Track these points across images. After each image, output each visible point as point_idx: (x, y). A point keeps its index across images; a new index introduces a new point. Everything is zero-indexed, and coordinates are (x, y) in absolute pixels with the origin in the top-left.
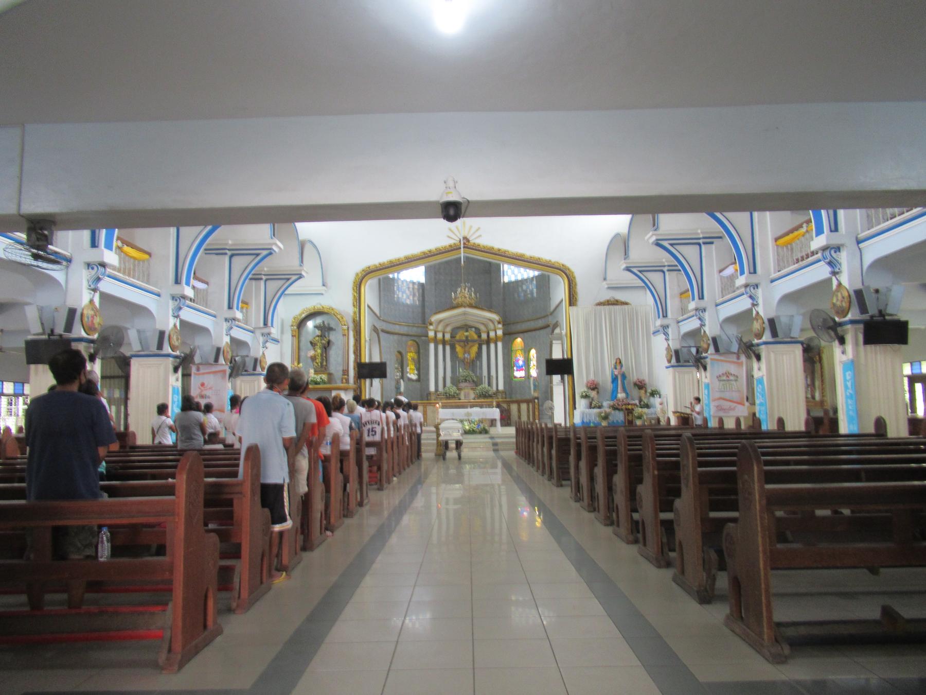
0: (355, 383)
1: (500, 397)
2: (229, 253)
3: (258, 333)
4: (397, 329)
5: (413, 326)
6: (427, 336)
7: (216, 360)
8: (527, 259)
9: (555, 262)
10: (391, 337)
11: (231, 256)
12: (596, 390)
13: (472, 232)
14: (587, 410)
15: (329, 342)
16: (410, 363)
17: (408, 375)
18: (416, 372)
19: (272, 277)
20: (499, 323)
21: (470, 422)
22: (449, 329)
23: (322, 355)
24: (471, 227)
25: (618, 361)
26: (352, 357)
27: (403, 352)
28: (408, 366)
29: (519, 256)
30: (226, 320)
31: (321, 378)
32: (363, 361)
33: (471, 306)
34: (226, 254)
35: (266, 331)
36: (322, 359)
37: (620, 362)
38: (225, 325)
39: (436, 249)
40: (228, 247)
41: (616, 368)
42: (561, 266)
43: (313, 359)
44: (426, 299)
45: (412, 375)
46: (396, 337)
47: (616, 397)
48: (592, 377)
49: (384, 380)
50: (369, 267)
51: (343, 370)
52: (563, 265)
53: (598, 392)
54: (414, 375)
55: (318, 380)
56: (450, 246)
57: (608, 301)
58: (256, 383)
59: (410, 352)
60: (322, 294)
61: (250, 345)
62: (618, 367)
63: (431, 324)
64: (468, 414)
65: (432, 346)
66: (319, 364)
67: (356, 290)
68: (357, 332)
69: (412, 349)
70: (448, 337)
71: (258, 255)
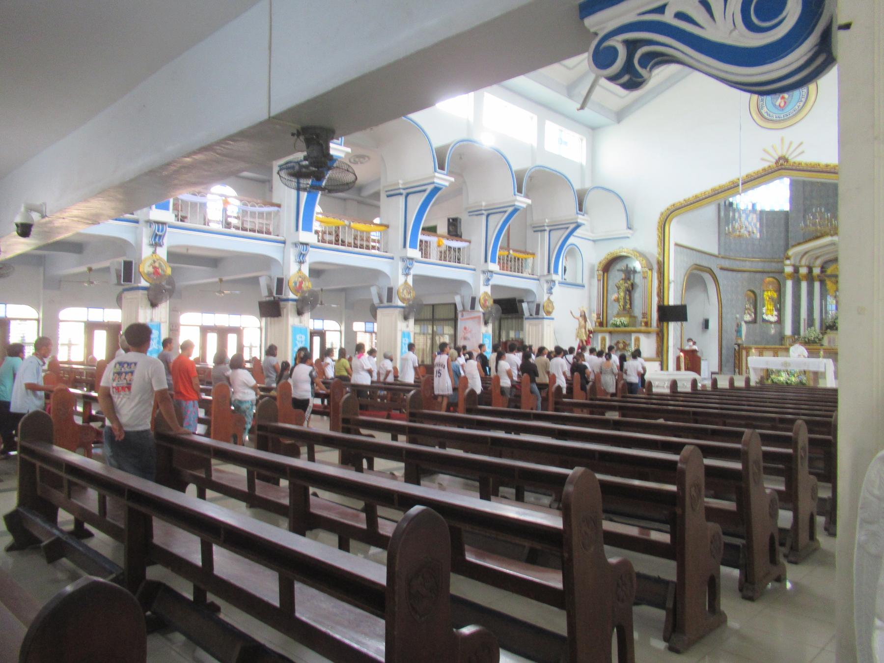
0: (658, 326)
2: (485, 213)
3: (543, 280)
4: (747, 266)
5: (771, 262)
6: (782, 272)
7: (473, 307)
10: (739, 275)
11: (488, 216)
13: (791, 149)
15: (632, 285)
16: (766, 302)
17: (764, 316)
18: (775, 313)
19: (554, 227)
21: (789, 373)
22: (819, 262)
23: (625, 298)
24: (791, 143)
26: (655, 300)
27: (757, 291)
28: (764, 306)
30: (484, 272)
31: (621, 321)
32: (666, 303)
34: (482, 214)
35: (548, 278)
36: (625, 303)
38: (482, 278)
39: (747, 176)
40: (483, 208)
43: (617, 300)
46: (746, 275)
49: (684, 323)
50: (674, 205)
51: (643, 313)
54: (772, 316)
55: (618, 323)
56: (764, 170)
58: (540, 326)
59: (767, 291)
60: (628, 237)
61: (536, 293)
63: (788, 258)
64: (786, 364)
65: (789, 284)
66: (622, 307)
67: (660, 230)
68: (661, 273)
69: (771, 287)
70: (817, 271)
71: (505, 212)
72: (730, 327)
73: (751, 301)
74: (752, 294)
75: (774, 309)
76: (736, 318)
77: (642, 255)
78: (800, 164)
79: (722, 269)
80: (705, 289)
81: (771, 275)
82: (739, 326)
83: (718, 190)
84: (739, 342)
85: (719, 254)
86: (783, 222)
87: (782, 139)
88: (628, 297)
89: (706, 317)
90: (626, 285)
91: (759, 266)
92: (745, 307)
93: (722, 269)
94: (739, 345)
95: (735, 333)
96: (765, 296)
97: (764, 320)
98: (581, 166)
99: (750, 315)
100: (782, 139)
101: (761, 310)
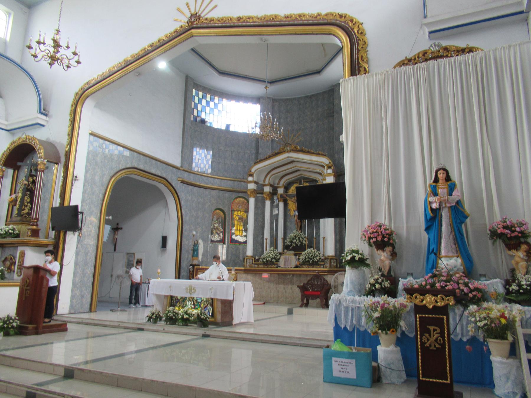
1: (327, 265)
5: (241, 181)
8: (281, 21)
9: (326, 15)
12: (388, 249)
14: (357, 298)
16: (236, 222)
17: (233, 237)
20: (329, 167)
21: (196, 303)
25: (441, 175)
27: (226, 210)
28: (234, 227)
29: (267, 21)
33: (297, 151)
37: (448, 178)
39: (159, 41)
41: (435, 194)
42: (338, 18)
44: (260, 152)
45: (239, 237)
46: (214, 192)
47: (435, 266)
48: (383, 219)
52: (341, 16)
53: (394, 255)
54: (241, 236)
56: (176, 31)
57: (425, 53)
59: (237, 211)
60: (43, 126)
62: (442, 190)
64: (191, 289)
69: (241, 207)
72: (188, 244)
73: (220, 221)
74: (222, 214)
75: (243, 229)
76: (193, 235)
77: (50, 146)
78: (212, 20)
79: (183, 182)
80: (166, 205)
81: (240, 195)
82: (196, 244)
84: (195, 262)
85: (181, 167)
86: (254, 144)
88: (27, 199)
89: (164, 235)
90: (26, 182)
91: (228, 185)
92: (214, 226)
93: (183, 182)
94: (193, 266)
95: (191, 252)
96: (235, 216)
97: (233, 241)
98: (5, 42)
99: (218, 234)
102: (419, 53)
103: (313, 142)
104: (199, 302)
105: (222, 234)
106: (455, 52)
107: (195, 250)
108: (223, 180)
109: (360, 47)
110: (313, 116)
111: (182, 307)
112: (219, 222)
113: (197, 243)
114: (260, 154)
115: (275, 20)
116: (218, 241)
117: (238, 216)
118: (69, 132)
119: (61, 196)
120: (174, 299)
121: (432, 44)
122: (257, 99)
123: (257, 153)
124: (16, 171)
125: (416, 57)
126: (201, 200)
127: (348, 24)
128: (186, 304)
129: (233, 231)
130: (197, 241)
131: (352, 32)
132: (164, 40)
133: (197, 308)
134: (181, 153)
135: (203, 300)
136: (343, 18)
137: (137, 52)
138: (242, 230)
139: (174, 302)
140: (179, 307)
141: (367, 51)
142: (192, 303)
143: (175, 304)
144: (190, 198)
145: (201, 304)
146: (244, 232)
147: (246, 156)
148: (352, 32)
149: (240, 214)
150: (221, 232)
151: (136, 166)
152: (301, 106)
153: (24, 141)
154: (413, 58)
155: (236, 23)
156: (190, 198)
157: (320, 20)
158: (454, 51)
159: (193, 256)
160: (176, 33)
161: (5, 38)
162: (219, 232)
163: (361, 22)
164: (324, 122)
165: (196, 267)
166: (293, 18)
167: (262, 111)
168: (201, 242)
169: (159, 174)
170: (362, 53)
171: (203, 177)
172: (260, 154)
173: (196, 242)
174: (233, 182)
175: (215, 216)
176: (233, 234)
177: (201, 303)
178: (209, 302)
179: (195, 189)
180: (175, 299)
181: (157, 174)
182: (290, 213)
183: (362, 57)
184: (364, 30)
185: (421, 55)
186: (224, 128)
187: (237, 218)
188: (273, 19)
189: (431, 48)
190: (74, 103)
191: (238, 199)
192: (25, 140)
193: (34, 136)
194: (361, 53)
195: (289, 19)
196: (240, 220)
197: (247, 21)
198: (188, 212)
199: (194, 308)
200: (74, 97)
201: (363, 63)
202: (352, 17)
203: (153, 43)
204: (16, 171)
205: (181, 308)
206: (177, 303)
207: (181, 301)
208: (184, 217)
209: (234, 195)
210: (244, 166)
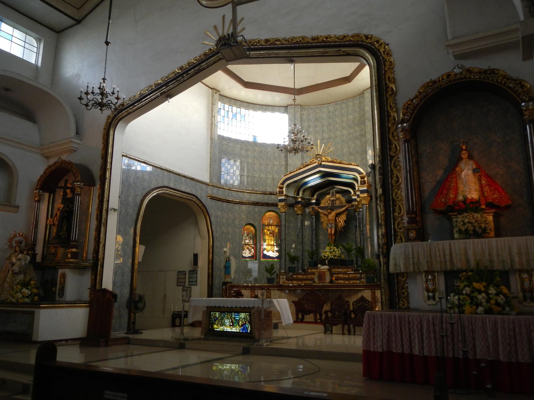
8: (308, 42)
9: (352, 37)
16: (267, 237)
17: (265, 252)
18: (276, 249)
27: (256, 224)
28: (265, 241)
39: (188, 64)
44: (289, 163)
46: (244, 207)
54: (273, 252)
56: (205, 54)
72: (219, 262)
73: (251, 236)
75: (275, 244)
76: (225, 252)
79: (213, 198)
81: (271, 208)
82: (228, 261)
83: (161, 83)
84: (228, 280)
87: (224, 17)
95: (223, 270)
97: (265, 256)
100: (224, 17)
101: (261, 245)
102: (443, 76)
103: (345, 150)
104: (237, 320)
105: (253, 250)
106: (478, 74)
107: (227, 268)
108: (252, 194)
109: (387, 68)
110: (344, 124)
111: (221, 325)
112: (250, 237)
113: (229, 260)
114: (290, 165)
115: (302, 43)
116: (249, 257)
117: (269, 230)
118: (102, 155)
119: (97, 218)
120: (212, 317)
121: (455, 67)
122: (285, 108)
123: (287, 165)
124: (52, 195)
125: (440, 79)
126: (231, 215)
127: (374, 45)
128: (225, 322)
129: (265, 247)
130: (229, 258)
131: (379, 53)
132: (193, 63)
133: (235, 326)
134: (209, 168)
135: (241, 318)
136: (370, 39)
137: (167, 75)
138: (274, 245)
139: (212, 319)
140: (217, 325)
141: (394, 71)
142: (230, 320)
143: (213, 322)
144: (220, 214)
145: (239, 322)
146: (275, 247)
147: (276, 168)
148: (379, 53)
149: (271, 229)
150: (252, 248)
151: (167, 185)
152: (330, 114)
153: (60, 165)
154: (437, 80)
155: (264, 45)
156: (220, 214)
157: (346, 41)
158: (476, 73)
159: (225, 274)
160: (205, 56)
161: (36, 64)
162: (250, 248)
163: (387, 43)
164: (355, 130)
165: (228, 285)
166: (320, 40)
167: (290, 120)
168: (232, 258)
169: (189, 192)
170: (389, 74)
171: (233, 192)
172: (290, 165)
173: (228, 259)
174: (262, 195)
175: (245, 232)
176: (264, 249)
177: (239, 320)
178: (247, 319)
179: (225, 204)
180: (214, 317)
181: (186, 191)
182: (323, 226)
183: (389, 77)
184: (390, 50)
185: (445, 77)
186: (251, 140)
187: (268, 233)
188: (300, 41)
189: (455, 70)
190: (107, 126)
191: (268, 213)
192: (60, 164)
193: (69, 160)
194: (388, 73)
195: (316, 41)
196: (272, 235)
197: (275, 43)
198: (218, 229)
199: (233, 325)
200: (106, 121)
201: (390, 83)
202: (378, 38)
203: (182, 66)
204: (52, 195)
205: (219, 326)
206: (215, 321)
207: (219, 319)
208: (214, 234)
209: (265, 208)
210: (273, 178)
